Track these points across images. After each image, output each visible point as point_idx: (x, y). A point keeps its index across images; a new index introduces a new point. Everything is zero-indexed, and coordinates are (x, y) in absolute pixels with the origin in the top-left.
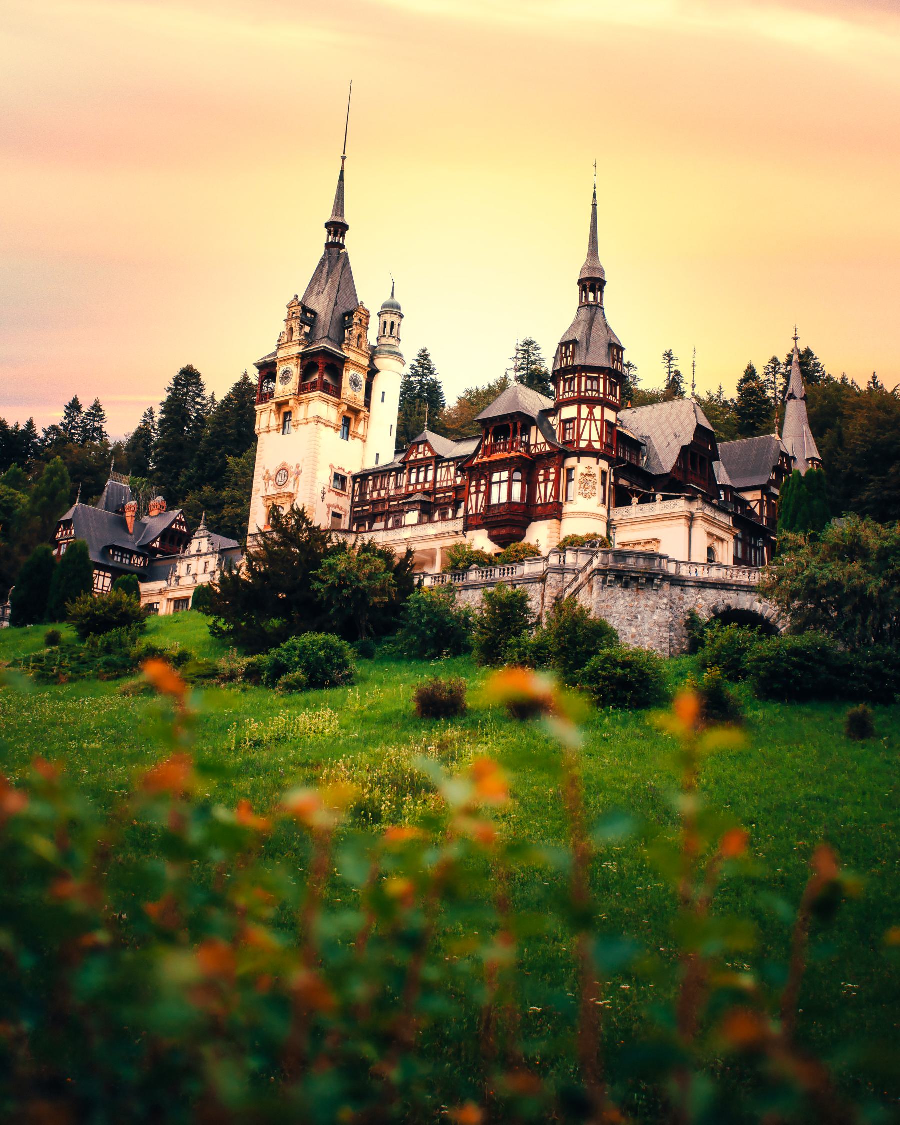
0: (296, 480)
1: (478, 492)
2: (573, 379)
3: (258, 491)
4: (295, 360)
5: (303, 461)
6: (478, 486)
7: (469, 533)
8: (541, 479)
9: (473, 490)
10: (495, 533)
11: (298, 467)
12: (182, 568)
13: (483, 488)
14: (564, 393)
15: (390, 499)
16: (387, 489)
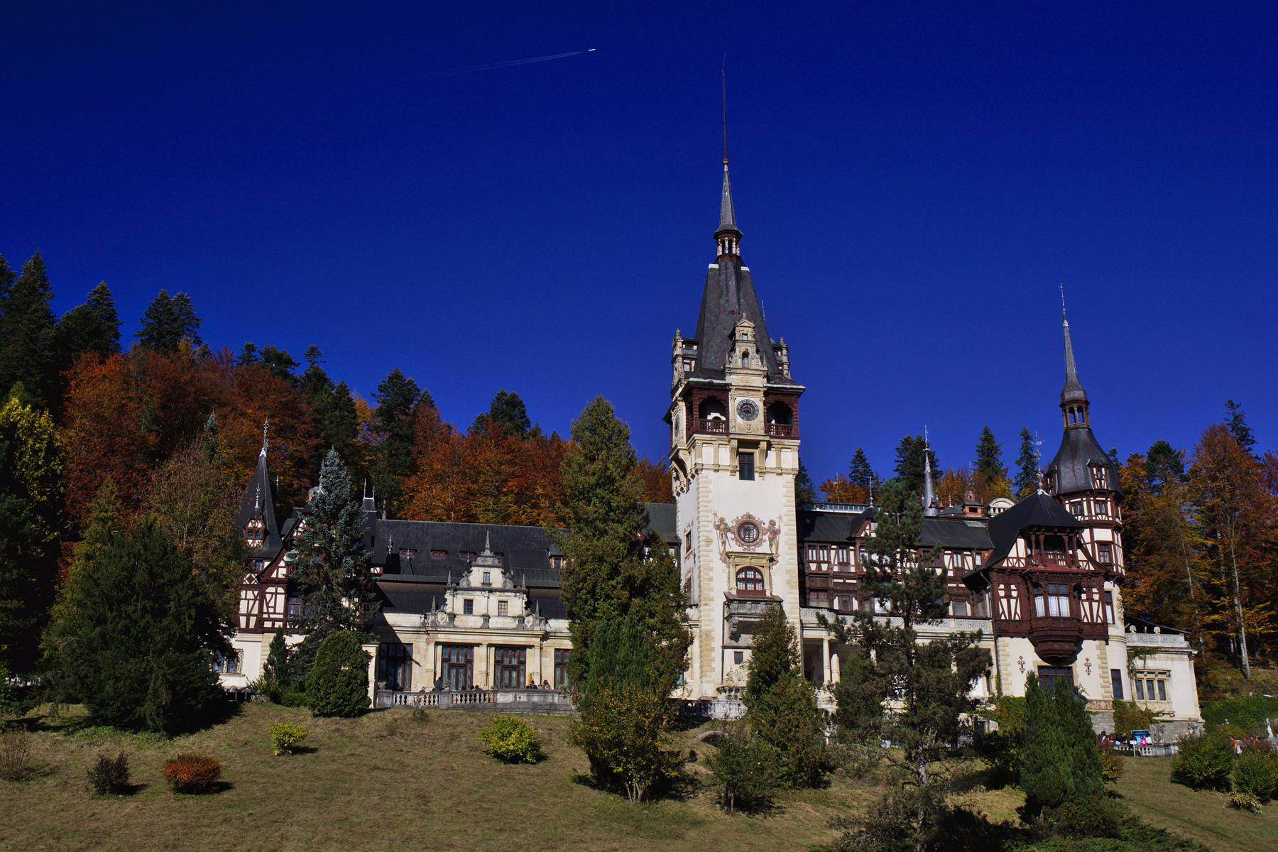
0: (771, 540)
1: (1008, 597)
2: (1105, 502)
3: (709, 541)
4: (761, 394)
5: (780, 518)
6: (1008, 590)
7: (1003, 641)
8: (1084, 596)
9: (1002, 593)
10: (1045, 647)
11: (772, 523)
12: (455, 603)
13: (1014, 594)
14: (1097, 514)
15: (837, 576)
16: (828, 562)
